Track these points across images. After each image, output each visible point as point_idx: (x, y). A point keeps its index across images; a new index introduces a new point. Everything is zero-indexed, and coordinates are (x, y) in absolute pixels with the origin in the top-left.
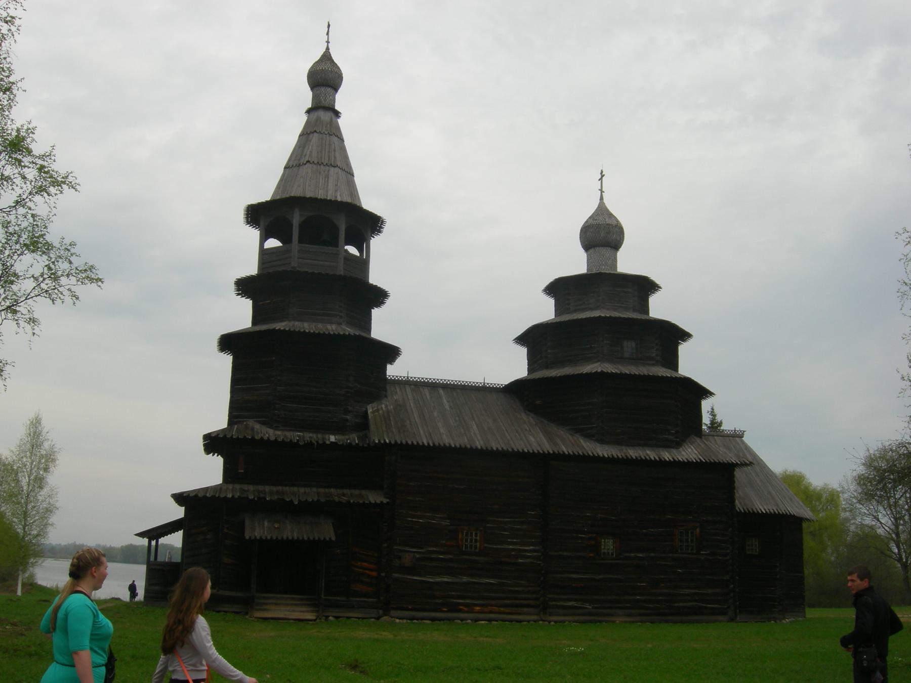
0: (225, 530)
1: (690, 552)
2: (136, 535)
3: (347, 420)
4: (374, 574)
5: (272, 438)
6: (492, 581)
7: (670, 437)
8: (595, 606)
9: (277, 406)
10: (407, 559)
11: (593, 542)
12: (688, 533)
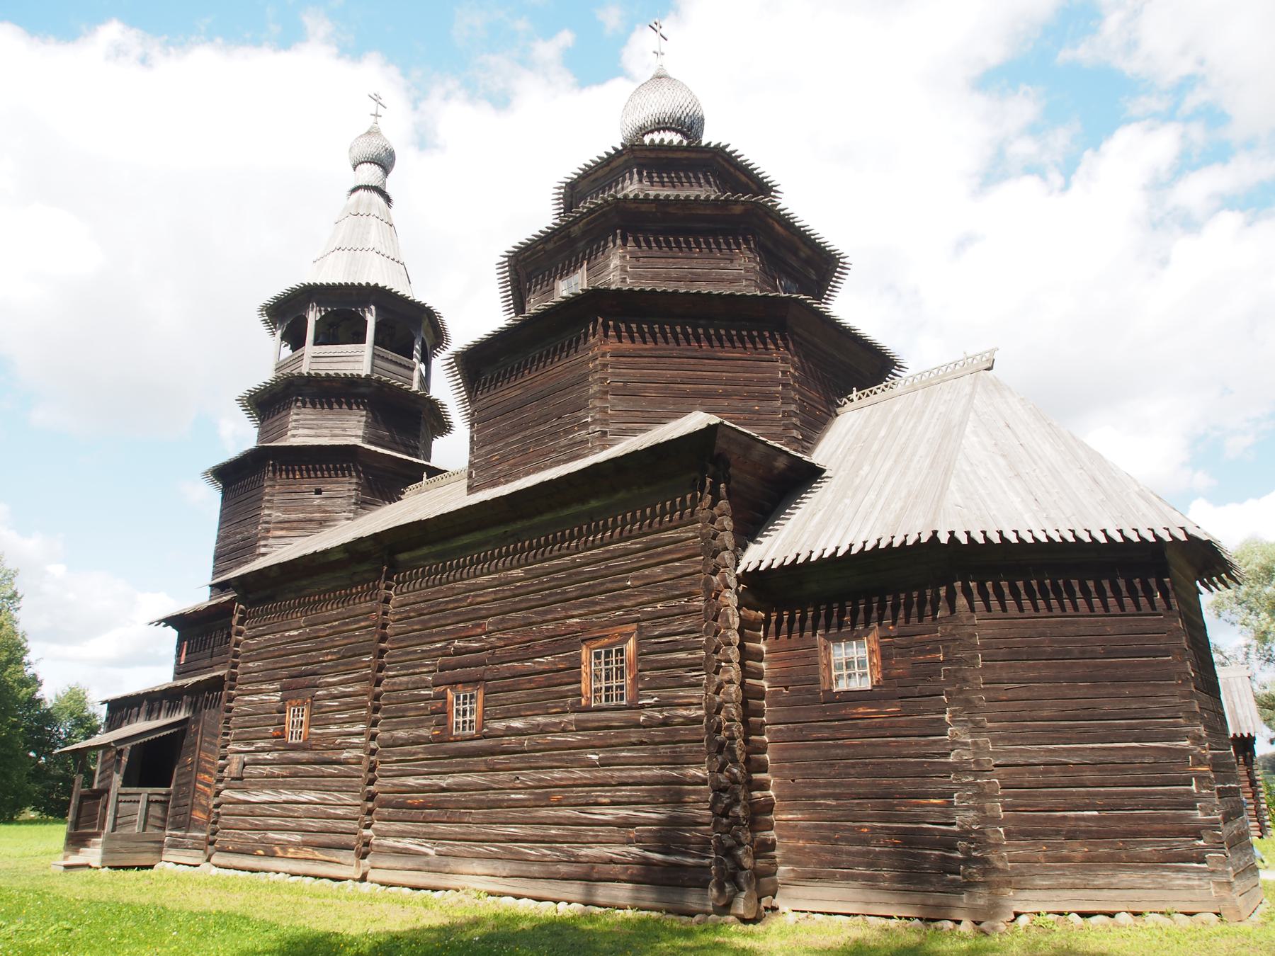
11: (439, 703)
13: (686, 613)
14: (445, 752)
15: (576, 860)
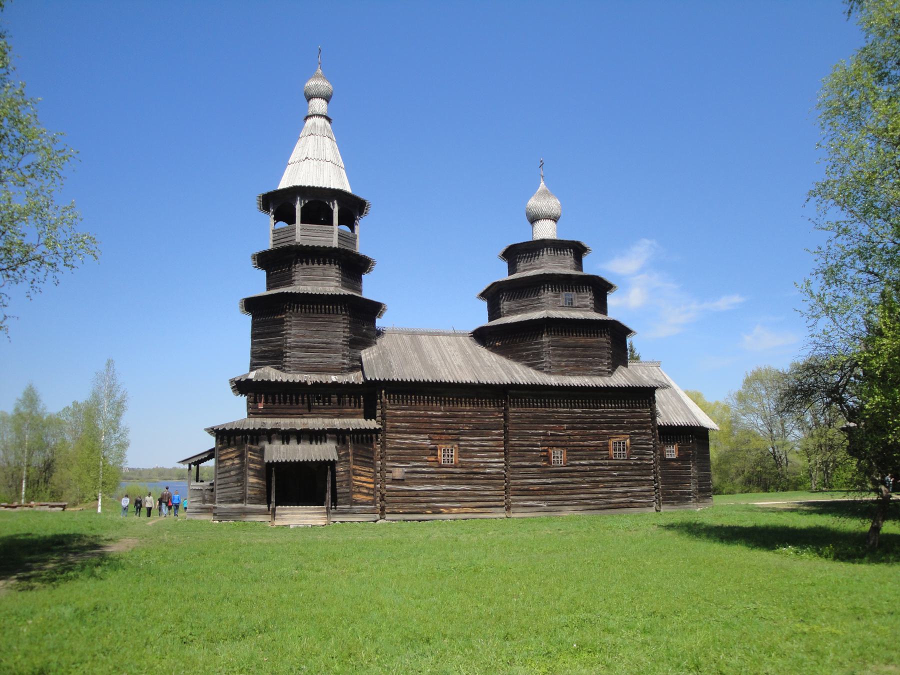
0: (249, 456)
1: (622, 458)
2: (180, 462)
3: (344, 364)
4: (372, 486)
5: (285, 380)
6: (466, 487)
7: (604, 368)
8: (549, 504)
9: (288, 354)
10: (398, 473)
11: (545, 454)
12: (620, 443)
13: (645, 434)
14: (548, 471)
15: (610, 503)
